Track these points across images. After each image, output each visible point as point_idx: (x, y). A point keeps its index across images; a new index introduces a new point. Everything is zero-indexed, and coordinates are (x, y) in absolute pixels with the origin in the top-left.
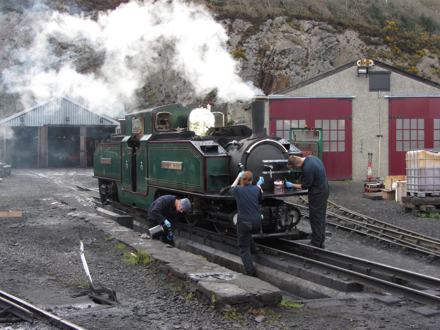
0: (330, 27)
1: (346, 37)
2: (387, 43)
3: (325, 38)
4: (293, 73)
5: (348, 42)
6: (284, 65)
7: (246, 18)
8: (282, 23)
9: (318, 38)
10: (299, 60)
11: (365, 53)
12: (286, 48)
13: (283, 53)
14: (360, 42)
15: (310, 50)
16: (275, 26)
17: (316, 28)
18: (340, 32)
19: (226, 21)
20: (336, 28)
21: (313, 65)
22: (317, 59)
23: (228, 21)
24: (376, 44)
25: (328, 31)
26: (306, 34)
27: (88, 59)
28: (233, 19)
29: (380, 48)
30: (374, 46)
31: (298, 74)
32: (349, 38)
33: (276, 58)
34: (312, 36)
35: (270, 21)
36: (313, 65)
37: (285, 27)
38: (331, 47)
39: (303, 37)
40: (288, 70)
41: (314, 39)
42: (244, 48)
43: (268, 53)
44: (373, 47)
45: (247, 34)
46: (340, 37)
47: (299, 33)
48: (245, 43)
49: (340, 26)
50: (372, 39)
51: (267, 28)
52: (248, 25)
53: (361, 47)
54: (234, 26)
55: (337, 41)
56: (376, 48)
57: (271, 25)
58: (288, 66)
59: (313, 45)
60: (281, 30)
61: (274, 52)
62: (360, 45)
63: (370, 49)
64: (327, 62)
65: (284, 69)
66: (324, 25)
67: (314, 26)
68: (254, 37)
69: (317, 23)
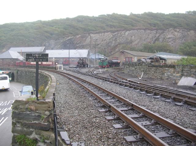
0: (186, 30)
5: (191, 34)
6: (169, 41)
8: (172, 30)
9: (181, 33)
13: (169, 38)
15: (177, 37)
17: (181, 31)
18: (189, 31)
23: (156, 31)
26: (177, 33)
31: (172, 43)
35: (168, 30)
37: (172, 31)
39: (176, 33)
41: (179, 34)
43: (166, 38)
46: (189, 33)
47: (175, 32)
51: (167, 31)
54: (157, 32)
57: (168, 30)
59: (179, 35)
66: (184, 30)
67: (180, 30)
68: (163, 34)
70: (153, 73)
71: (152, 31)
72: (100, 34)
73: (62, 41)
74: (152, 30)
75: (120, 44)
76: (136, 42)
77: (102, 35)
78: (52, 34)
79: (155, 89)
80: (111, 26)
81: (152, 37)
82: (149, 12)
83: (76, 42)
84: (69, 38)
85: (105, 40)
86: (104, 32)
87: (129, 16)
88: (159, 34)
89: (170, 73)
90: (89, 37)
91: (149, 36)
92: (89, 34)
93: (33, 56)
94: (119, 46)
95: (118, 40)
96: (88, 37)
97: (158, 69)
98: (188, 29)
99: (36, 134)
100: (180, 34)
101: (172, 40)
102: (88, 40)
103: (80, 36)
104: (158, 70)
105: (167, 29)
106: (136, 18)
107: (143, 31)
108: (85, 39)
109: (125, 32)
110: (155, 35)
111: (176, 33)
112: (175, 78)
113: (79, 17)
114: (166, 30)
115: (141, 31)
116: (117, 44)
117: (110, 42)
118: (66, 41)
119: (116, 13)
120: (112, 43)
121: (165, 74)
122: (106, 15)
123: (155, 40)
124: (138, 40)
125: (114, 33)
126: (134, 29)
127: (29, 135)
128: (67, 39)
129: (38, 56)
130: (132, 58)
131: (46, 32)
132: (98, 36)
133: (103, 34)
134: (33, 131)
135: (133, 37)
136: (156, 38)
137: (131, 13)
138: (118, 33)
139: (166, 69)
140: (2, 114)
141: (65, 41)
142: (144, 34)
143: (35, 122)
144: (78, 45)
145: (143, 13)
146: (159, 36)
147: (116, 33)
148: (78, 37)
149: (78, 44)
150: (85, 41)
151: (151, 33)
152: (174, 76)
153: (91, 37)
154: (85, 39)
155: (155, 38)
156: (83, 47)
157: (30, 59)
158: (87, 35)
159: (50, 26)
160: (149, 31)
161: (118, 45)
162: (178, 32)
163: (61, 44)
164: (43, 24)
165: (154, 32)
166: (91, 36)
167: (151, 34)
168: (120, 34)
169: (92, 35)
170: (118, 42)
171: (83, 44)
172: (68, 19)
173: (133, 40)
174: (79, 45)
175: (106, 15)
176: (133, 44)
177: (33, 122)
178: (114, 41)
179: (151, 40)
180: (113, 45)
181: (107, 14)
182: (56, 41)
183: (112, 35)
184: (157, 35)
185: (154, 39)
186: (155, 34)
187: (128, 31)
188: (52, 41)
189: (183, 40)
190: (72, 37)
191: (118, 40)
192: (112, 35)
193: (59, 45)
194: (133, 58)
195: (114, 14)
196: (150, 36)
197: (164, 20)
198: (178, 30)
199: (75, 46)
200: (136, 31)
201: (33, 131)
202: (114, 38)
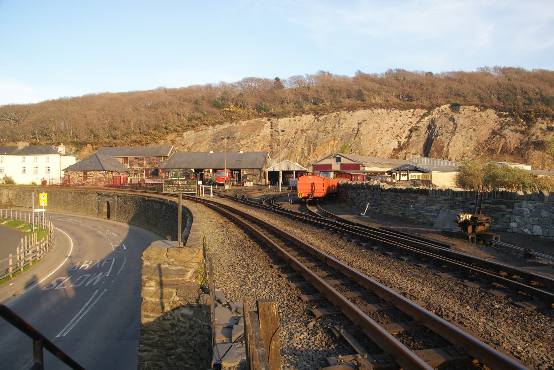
0: (476, 108)
2: (512, 115)
7: (423, 107)
14: (496, 116)
18: (482, 111)
23: (412, 110)
24: (506, 116)
25: (475, 111)
28: (415, 109)
29: (508, 119)
35: (438, 108)
44: (503, 119)
45: (423, 117)
46: (483, 114)
50: (504, 113)
54: (415, 113)
64: (472, 130)
66: (473, 108)
70: (390, 203)
71: (402, 112)
72: (292, 118)
79: (373, 233)
89: (419, 203)
90: (269, 123)
97: (398, 196)
103: (247, 121)
104: (398, 198)
110: (410, 120)
112: (427, 214)
115: (380, 110)
118: (220, 134)
123: (411, 131)
125: (321, 115)
129: (182, 184)
133: (298, 118)
137: (359, 72)
139: (412, 197)
140: (95, 284)
141: (217, 133)
142: (386, 119)
146: (417, 122)
151: (401, 116)
152: (427, 211)
153: (271, 126)
155: (410, 127)
158: (264, 120)
169: (274, 120)
171: (255, 140)
173: (362, 131)
175: (305, 76)
177: (173, 279)
179: (402, 131)
181: (307, 75)
182: (198, 133)
184: (414, 120)
185: (408, 128)
188: (188, 132)
191: (331, 132)
196: (399, 123)
199: (238, 144)
200: (368, 111)
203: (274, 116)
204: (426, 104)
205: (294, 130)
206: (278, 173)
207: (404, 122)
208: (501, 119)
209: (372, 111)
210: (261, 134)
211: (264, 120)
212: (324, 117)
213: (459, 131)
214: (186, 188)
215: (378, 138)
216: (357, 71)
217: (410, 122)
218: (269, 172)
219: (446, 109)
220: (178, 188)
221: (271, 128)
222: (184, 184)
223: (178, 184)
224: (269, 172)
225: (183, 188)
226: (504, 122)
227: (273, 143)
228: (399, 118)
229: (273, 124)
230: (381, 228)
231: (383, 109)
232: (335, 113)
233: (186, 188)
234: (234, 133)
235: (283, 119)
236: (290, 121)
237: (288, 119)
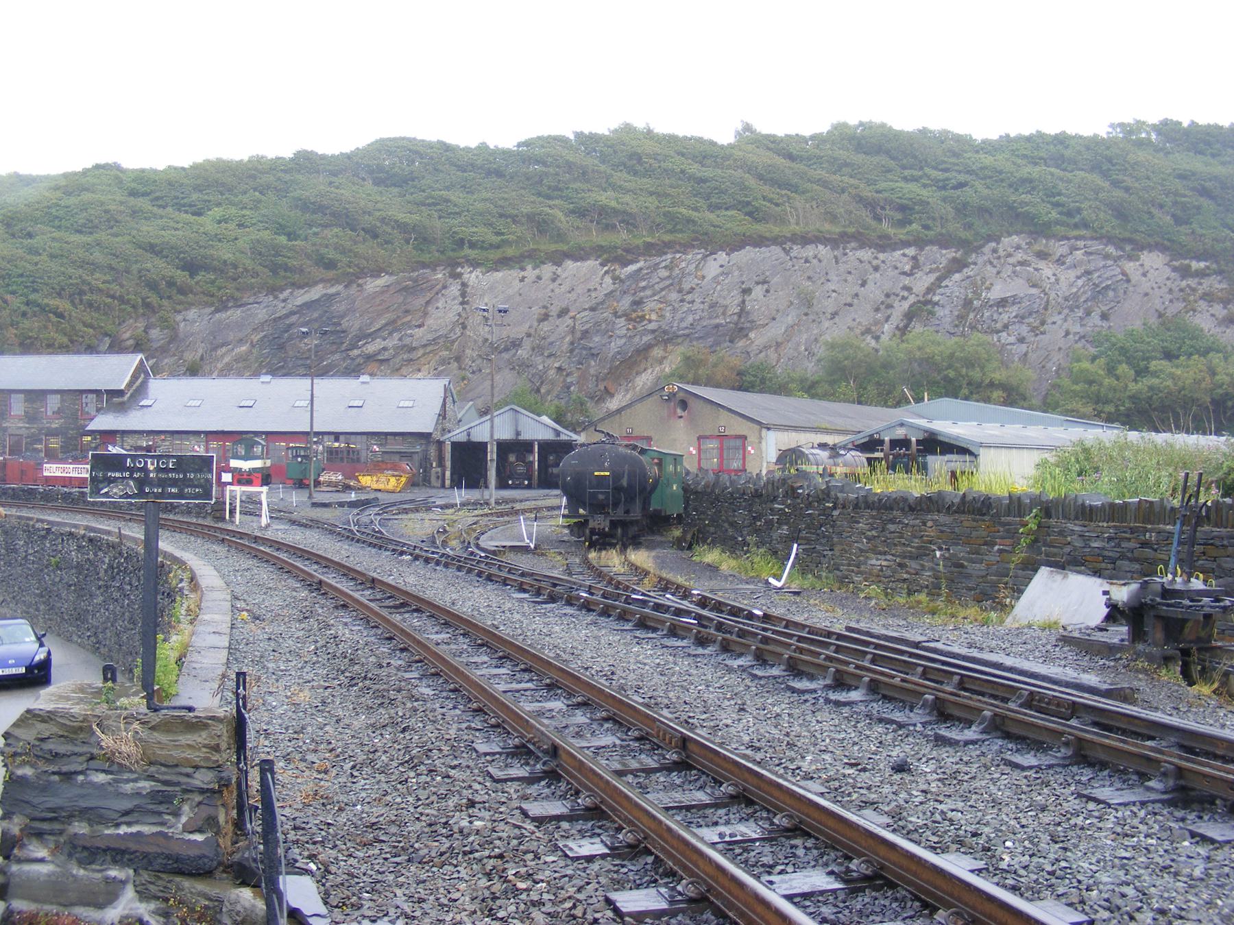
0: (1111, 249)
1: (1142, 265)
3: (1097, 270)
4: (1012, 339)
5: (1144, 275)
7: (944, 242)
8: (1018, 247)
9: (1079, 271)
10: (1030, 314)
11: (1177, 294)
12: (1009, 294)
13: (1002, 303)
14: (1167, 271)
15: (1052, 296)
16: (1001, 253)
17: (1079, 254)
18: (1130, 258)
19: (907, 251)
20: (1122, 249)
21: (1054, 323)
22: (1066, 311)
23: (911, 251)
24: (1201, 274)
25: (1107, 257)
27: (653, 331)
30: (1196, 280)
31: (1021, 340)
32: (1147, 268)
33: (987, 314)
34: (1068, 268)
35: (994, 244)
36: (1054, 323)
37: (1020, 256)
38: (1107, 287)
40: (1004, 334)
42: (936, 298)
44: (1192, 282)
46: (1130, 267)
47: (1041, 264)
48: (940, 287)
49: (1134, 246)
50: (1195, 265)
52: (947, 255)
53: (1168, 283)
54: (921, 259)
55: (1124, 273)
56: (1200, 284)
58: (1006, 327)
59: (1063, 284)
60: (1011, 260)
61: (987, 304)
62: (1168, 279)
63: (1188, 286)
65: (998, 332)
66: (1096, 246)
68: (957, 276)
69: (1081, 243)
71: (881, 256)
72: (530, 273)
73: (261, 313)
74: (882, 248)
75: (666, 338)
76: (776, 331)
77: (539, 278)
78: (192, 268)
80: (604, 217)
81: (888, 296)
82: (865, 119)
83: (357, 325)
84: (316, 293)
85: (563, 312)
86: (558, 258)
87: (731, 146)
88: (932, 278)
90: (454, 289)
91: (863, 284)
92: (459, 264)
93: (132, 470)
94: (657, 352)
95: (654, 317)
96: (445, 287)
97: (892, 521)
98: (1130, 241)
99: (143, 895)
100: (1072, 274)
101: (1021, 318)
102: (444, 313)
103: (384, 280)
105: (989, 238)
106: (780, 161)
107: (823, 250)
108: (421, 301)
109: (705, 257)
110: (907, 281)
111: (1047, 270)
113: (384, 147)
114: (977, 249)
115: (810, 251)
116: (645, 339)
117: (597, 324)
118: (294, 319)
119: (639, 124)
120: (609, 333)
121: (938, 554)
122: (572, 137)
123: (910, 316)
124: (790, 320)
126: (759, 241)
127: (100, 906)
128: (299, 301)
129: (158, 470)
130: (745, 438)
131: (152, 249)
132: (517, 283)
133: (548, 270)
134: (123, 883)
135: (758, 291)
136: (912, 299)
137: (748, 128)
138: (656, 267)
141: (287, 316)
142: (832, 276)
143: (134, 829)
144: (371, 348)
145: (823, 127)
146: (929, 290)
147: (641, 264)
148: (373, 285)
149: (373, 336)
150: (426, 314)
151: (876, 269)
153: (463, 295)
154: (421, 301)
155: (906, 305)
156: (398, 363)
157: (111, 481)
159: (179, 207)
160: (866, 254)
161: (648, 347)
162: (1060, 261)
163: (256, 338)
164: (133, 193)
165: (900, 258)
166: (464, 285)
167: (878, 275)
168: (664, 273)
169: (473, 277)
170: (651, 326)
171: (407, 341)
172: (306, 162)
173: (754, 317)
174: (383, 344)
175: (572, 137)
176: (758, 338)
177: (123, 830)
178: (622, 322)
180: (615, 346)
181: (579, 135)
183: (615, 278)
184: (922, 282)
185: (901, 307)
186: (904, 273)
187: (722, 256)
188: (192, 313)
189: (1095, 318)
190: (332, 290)
192: (608, 280)
193: (241, 341)
194: (752, 438)
195: (628, 129)
196: (874, 292)
197: (967, 178)
198: (1060, 248)
199: (356, 352)
200: (776, 250)
201: (123, 883)
202: (625, 303)
203: (475, 264)
204: (955, 227)
205: (536, 310)
206: (482, 446)
207: (887, 286)
208: (1184, 283)
209: (787, 252)
210: (430, 322)
211: (440, 276)
212: (632, 268)
213: (1057, 318)
214: (174, 483)
215: (805, 336)
216: (740, 128)
217: (907, 288)
218: (453, 444)
219: (1018, 247)
220: (141, 483)
221: (462, 303)
222: (167, 470)
223: (144, 469)
224: (453, 444)
225: (162, 483)
226: (1194, 290)
227: (468, 352)
228: (873, 277)
229: (468, 290)
230: (849, 629)
231: (821, 247)
232: (669, 256)
233: (174, 483)
234: (342, 317)
235: (499, 275)
236: (522, 280)
237: (515, 273)
